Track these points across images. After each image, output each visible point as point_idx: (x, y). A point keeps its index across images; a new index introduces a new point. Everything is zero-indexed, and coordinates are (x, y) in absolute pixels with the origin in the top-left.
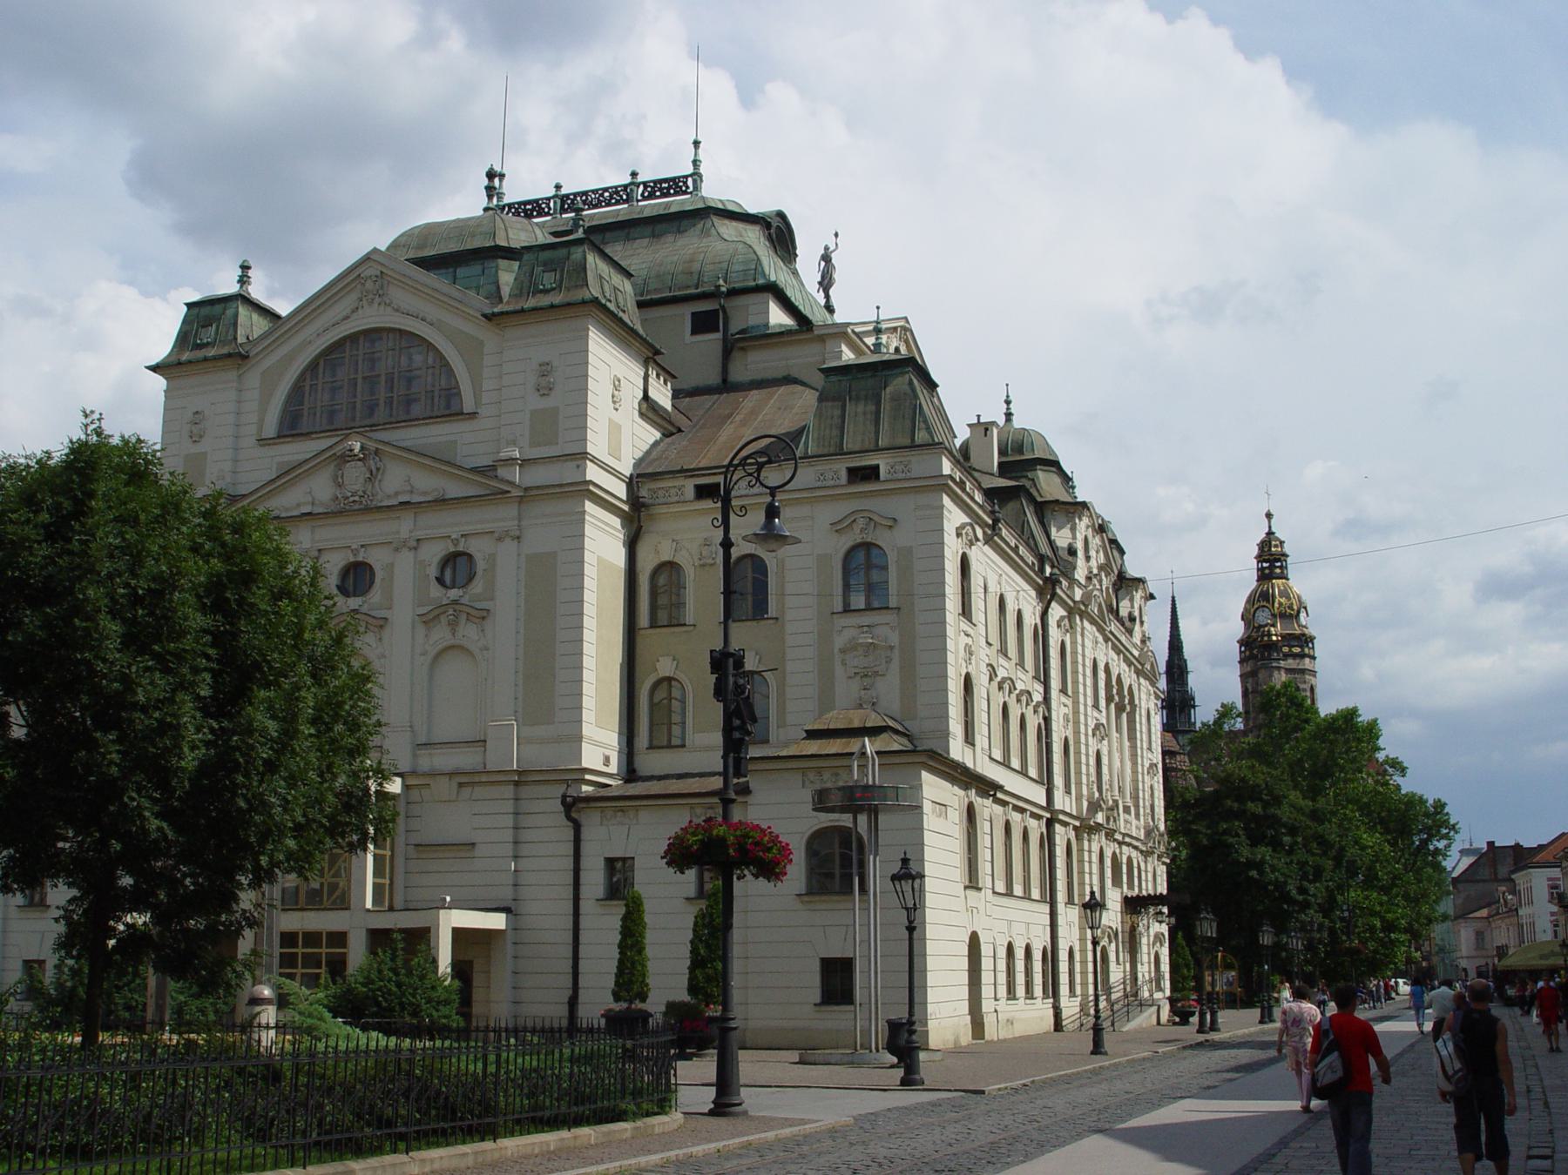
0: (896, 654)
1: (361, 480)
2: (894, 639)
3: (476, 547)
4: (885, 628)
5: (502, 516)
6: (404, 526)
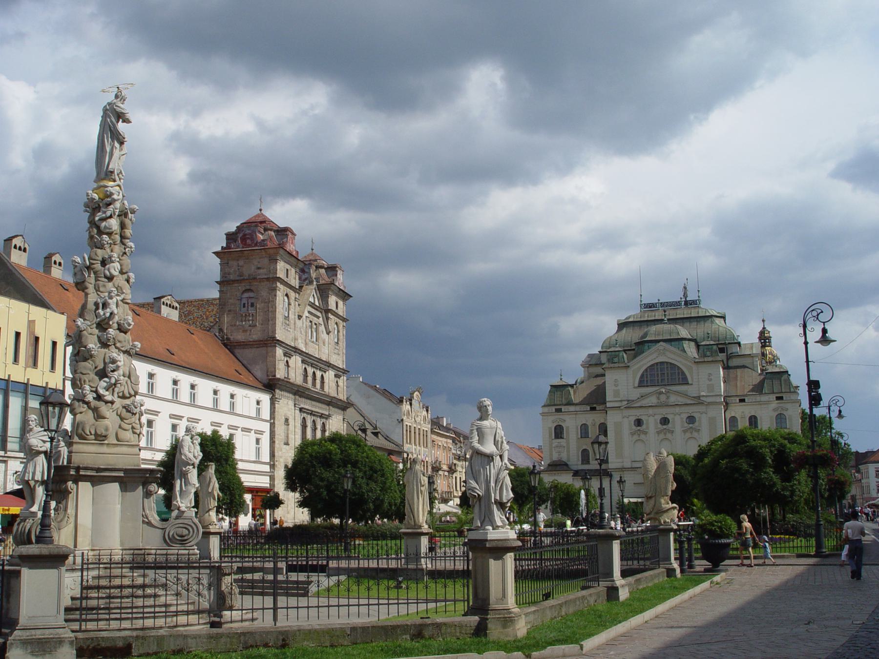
3: (696, 415)
5: (702, 408)
6: (677, 409)
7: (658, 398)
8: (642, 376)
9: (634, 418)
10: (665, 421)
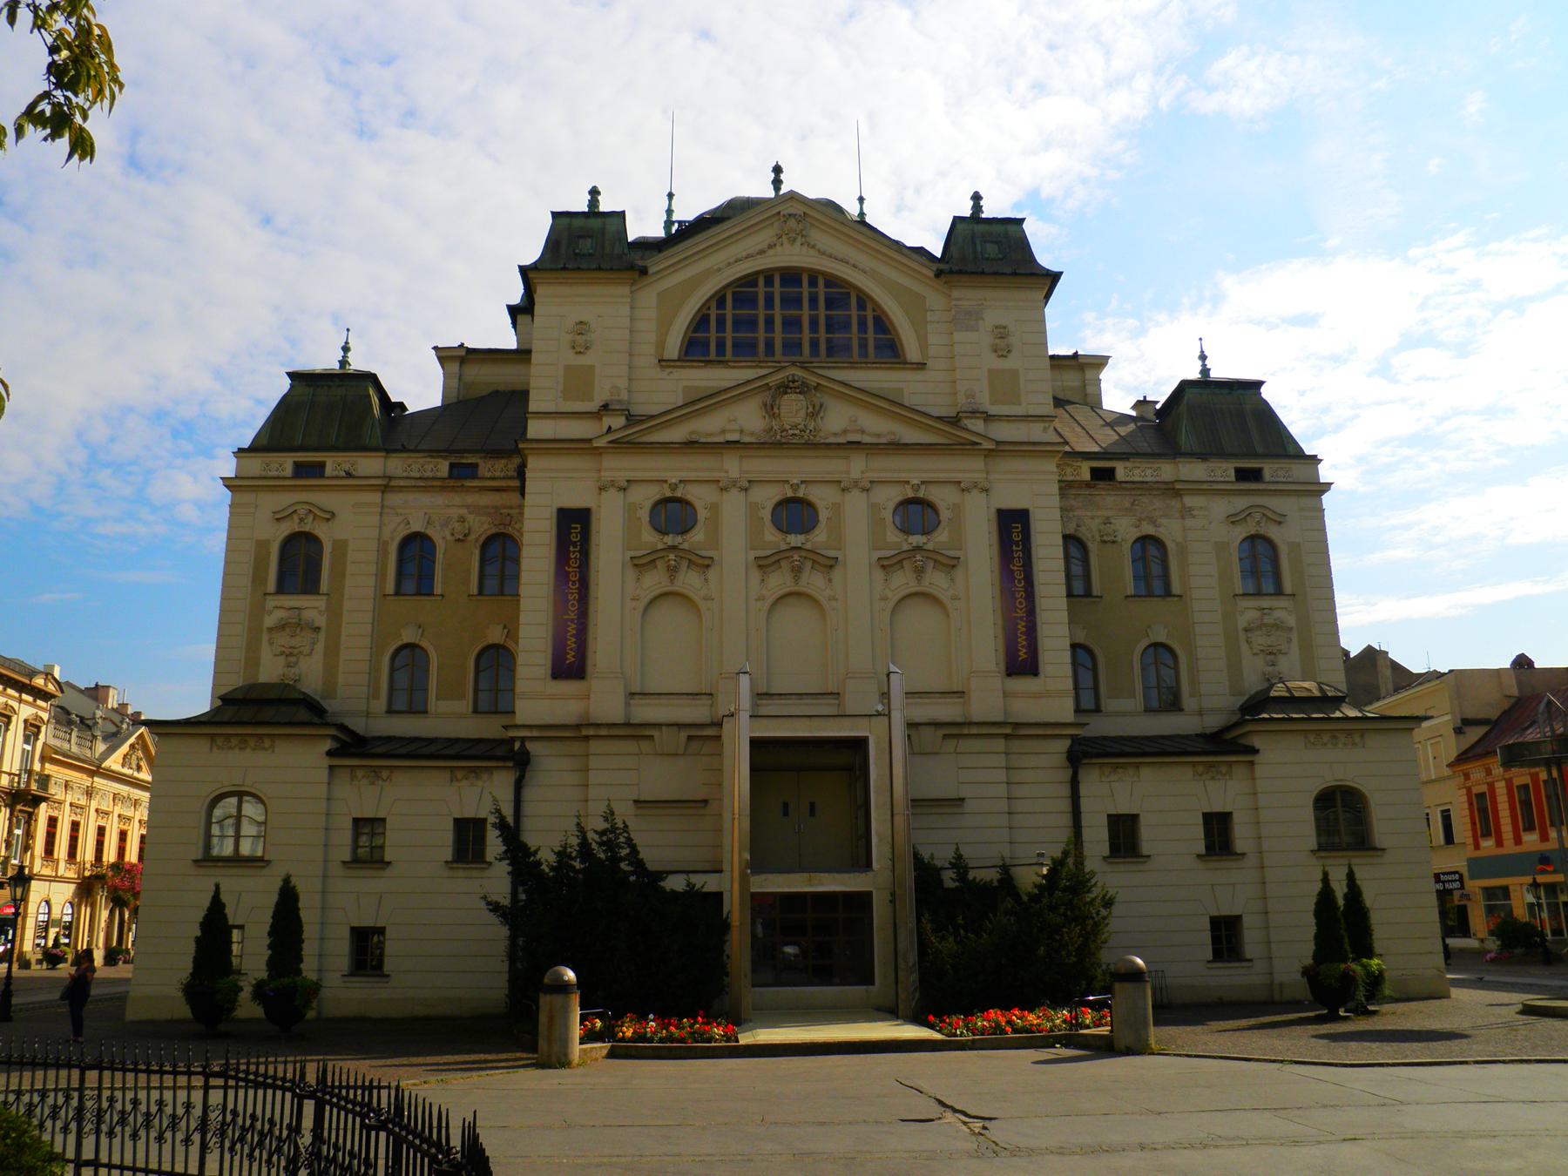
0: (1294, 636)
1: (802, 413)
2: (1291, 621)
4: (1282, 610)
5: (969, 468)
6: (857, 466)
7: (770, 410)
8: (701, 322)
9: (651, 494)
10: (795, 513)
